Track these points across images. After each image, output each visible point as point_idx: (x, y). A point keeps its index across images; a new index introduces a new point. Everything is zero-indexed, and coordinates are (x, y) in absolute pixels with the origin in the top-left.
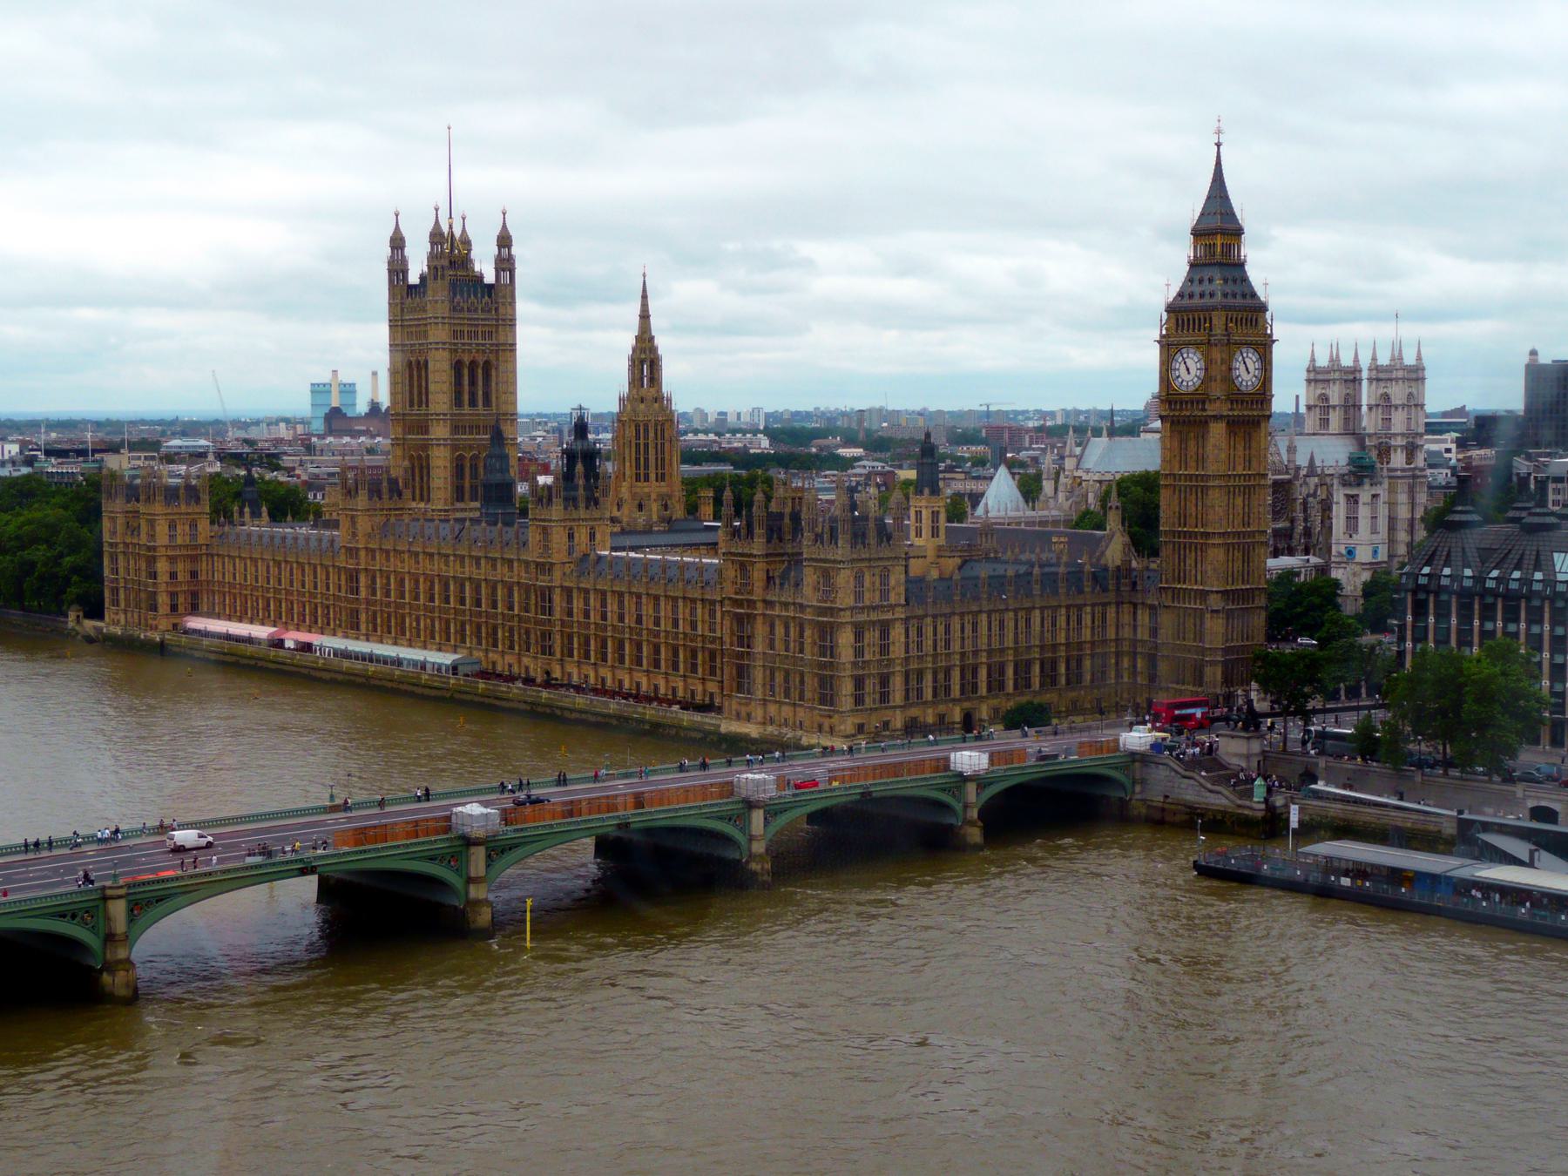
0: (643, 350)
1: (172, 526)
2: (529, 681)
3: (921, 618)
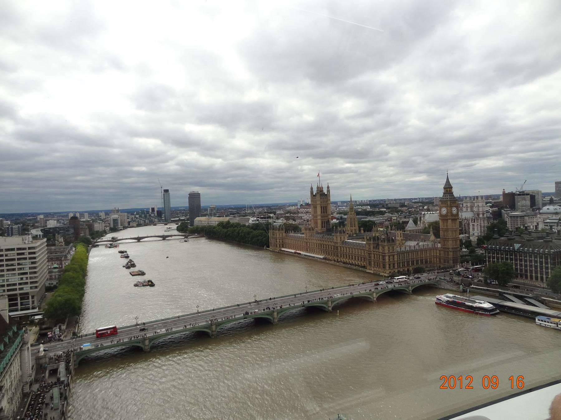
1: (279, 234)
2: (335, 261)
3: (399, 254)
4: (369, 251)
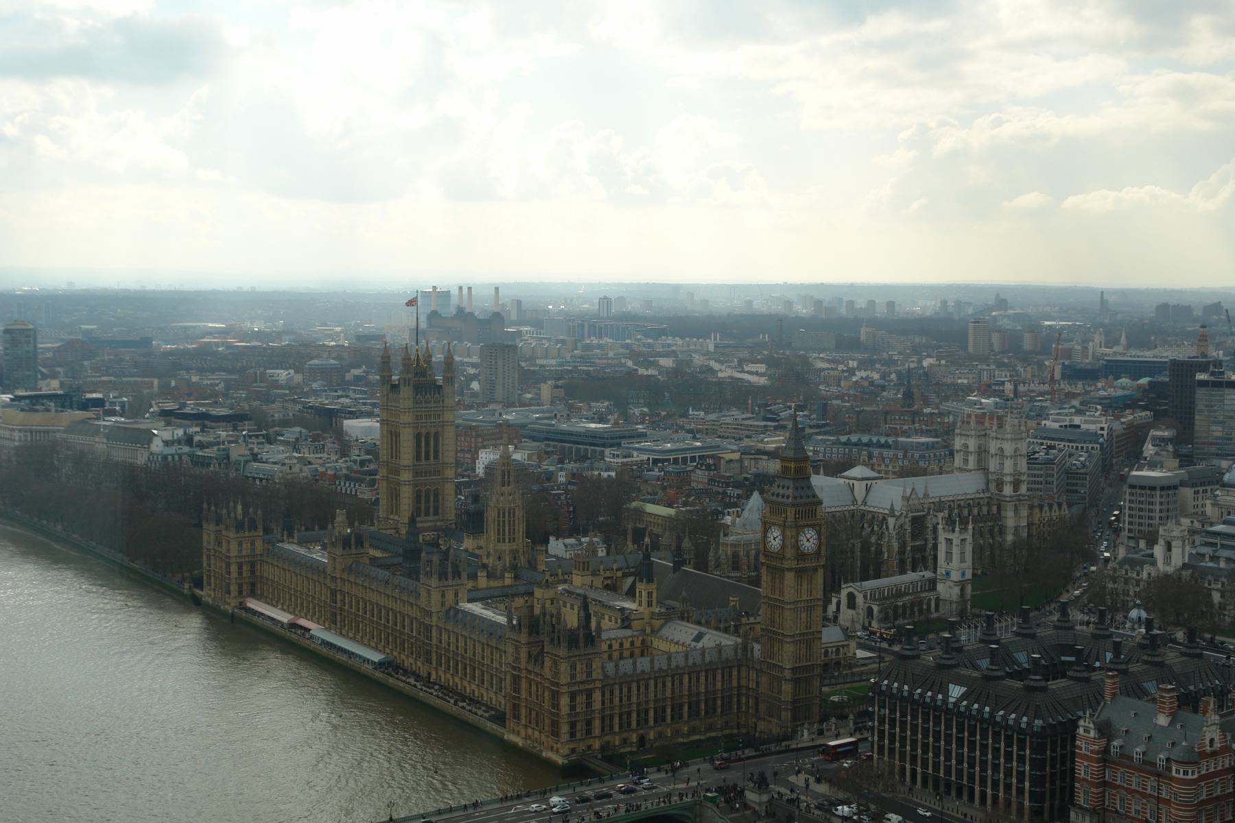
0: (504, 464)
1: (240, 544)
2: (418, 677)
4: (514, 668)
